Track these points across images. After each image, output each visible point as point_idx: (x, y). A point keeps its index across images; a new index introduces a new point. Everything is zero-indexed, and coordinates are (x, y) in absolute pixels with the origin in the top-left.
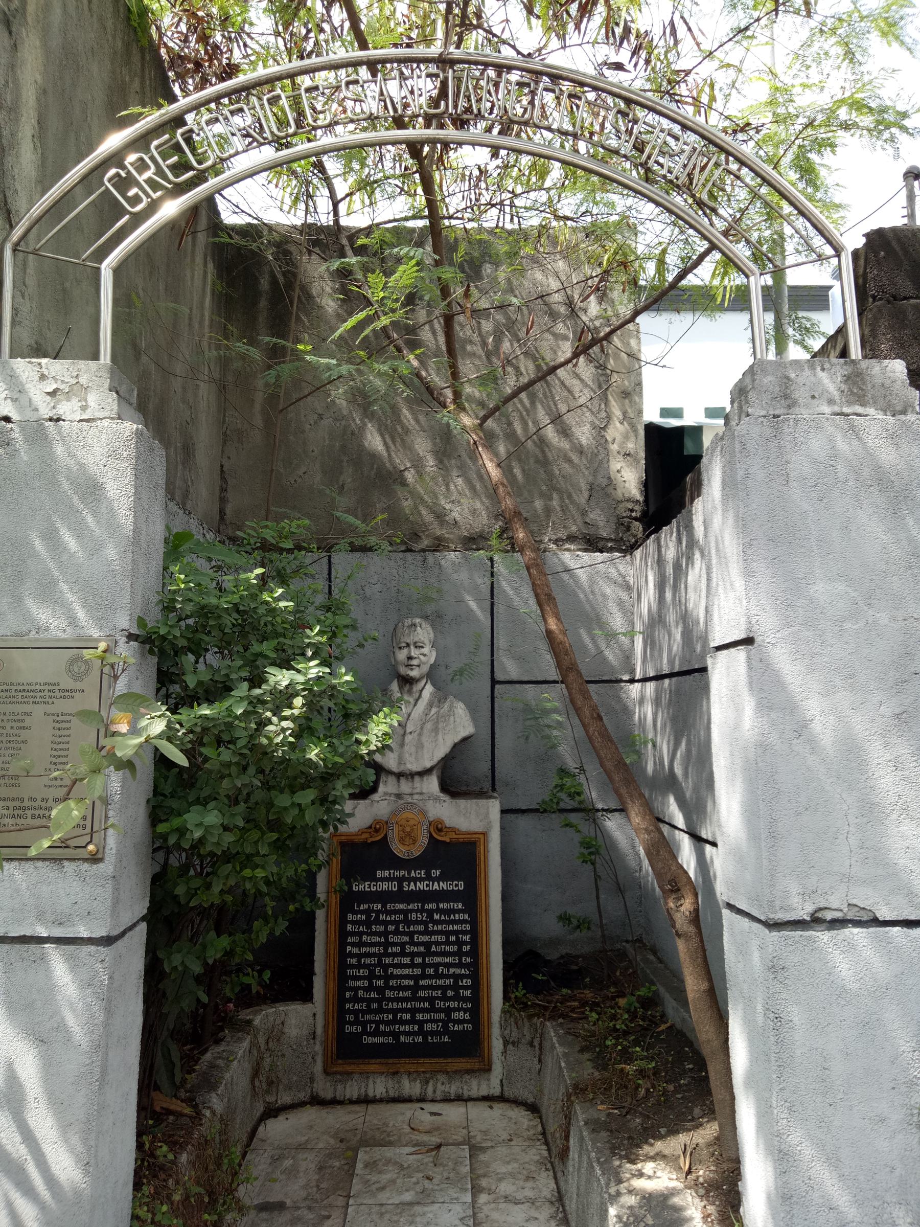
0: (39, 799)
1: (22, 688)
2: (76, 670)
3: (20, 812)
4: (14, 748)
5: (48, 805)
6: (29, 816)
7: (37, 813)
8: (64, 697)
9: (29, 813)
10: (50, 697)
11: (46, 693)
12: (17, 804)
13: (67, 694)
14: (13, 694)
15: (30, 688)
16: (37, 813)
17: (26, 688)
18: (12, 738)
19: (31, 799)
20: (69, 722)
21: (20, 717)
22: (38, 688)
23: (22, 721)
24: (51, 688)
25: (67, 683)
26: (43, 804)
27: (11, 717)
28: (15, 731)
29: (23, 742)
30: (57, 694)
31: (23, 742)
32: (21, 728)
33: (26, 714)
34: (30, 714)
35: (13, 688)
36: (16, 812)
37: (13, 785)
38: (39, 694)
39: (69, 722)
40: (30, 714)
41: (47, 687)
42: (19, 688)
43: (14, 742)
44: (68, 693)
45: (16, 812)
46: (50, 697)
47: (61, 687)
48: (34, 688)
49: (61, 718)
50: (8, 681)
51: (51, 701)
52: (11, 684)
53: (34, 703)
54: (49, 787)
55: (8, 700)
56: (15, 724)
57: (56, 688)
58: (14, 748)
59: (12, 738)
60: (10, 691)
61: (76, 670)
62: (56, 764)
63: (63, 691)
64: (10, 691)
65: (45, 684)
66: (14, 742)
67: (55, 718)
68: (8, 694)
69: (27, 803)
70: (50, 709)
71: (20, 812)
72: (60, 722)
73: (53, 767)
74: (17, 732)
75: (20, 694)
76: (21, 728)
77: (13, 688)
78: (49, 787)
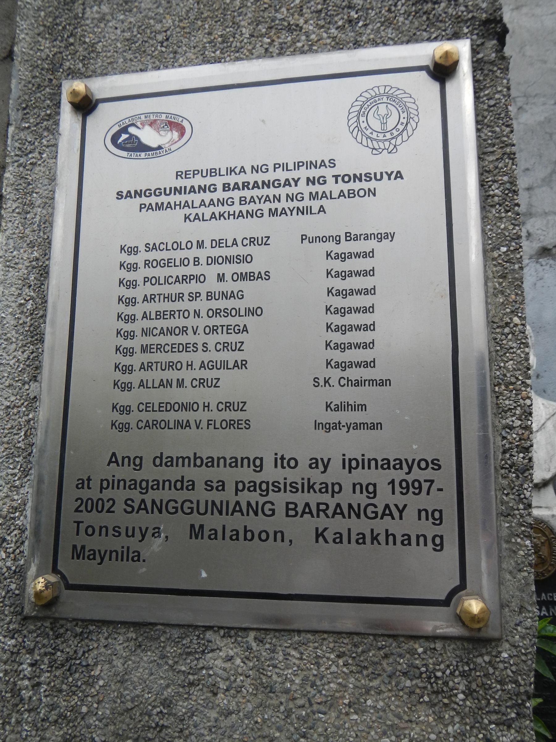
0: (304, 463)
1: (240, 179)
2: (376, 125)
3: (254, 497)
4: (228, 329)
5: (330, 477)
6: (280, 510)
7: (300, 499)
8: (352, 194)
9: (279, 499)
10: (313, 196)
11: (303, 188)
12: (246, 474)
13: (356, 186)
14: (220, 194)
15: (260, 177)
16: (300, 499)
17: (251, 178)
18: (222, 304)
19: (281, 461)
20: (370, 254)
21: (240, 250)
22: (281, 175)
23: (245, 259)
24: (314, 173)
25: (354, 157)
26: (317, 476)
27: (217, 252)
28: (229, 286)
29: (251, 312)
30: (331, 187)
31: (251, 312)
32: (243, 277)
33: (252, 241)
34: (265, 241)
35: (219, 181)
36: (245, 497)
37: (231, 424)
38: (283, 192)
39: (370, 254)
40: (265, 241)
41: (303, 173)
42: (232, 179)
43: (227, 313)
44: (358, 185)
45: (245, 497)
46: (313, 196)
47: (339, 170)
48: (270, 176)
49: (346, 247)
50: (205, 166)
51: (316, 205)
52: (213, 172)
53: (273, 213)
54: (328, 427)
55: (208, 212)
56: (228, 269)
57: (328, 173)
58: (228, 329)
59: (222, 304)
60: (212, 188)
61: (376, 125)
62: (343, 366)
63: (347, 178)
64: (212, 188)
65: (298, 165)
66: (227, 313)
67: (331, 246)
68: (207, 197)
69: (270, 473)
70: (314, 225)
71: (254, 497)
72: (343, 257)
73: (335, 374)
74: (235, 287)
75: (236, 195)
76: (243, 277)
77: (219, 181)
78: (328, 427)
